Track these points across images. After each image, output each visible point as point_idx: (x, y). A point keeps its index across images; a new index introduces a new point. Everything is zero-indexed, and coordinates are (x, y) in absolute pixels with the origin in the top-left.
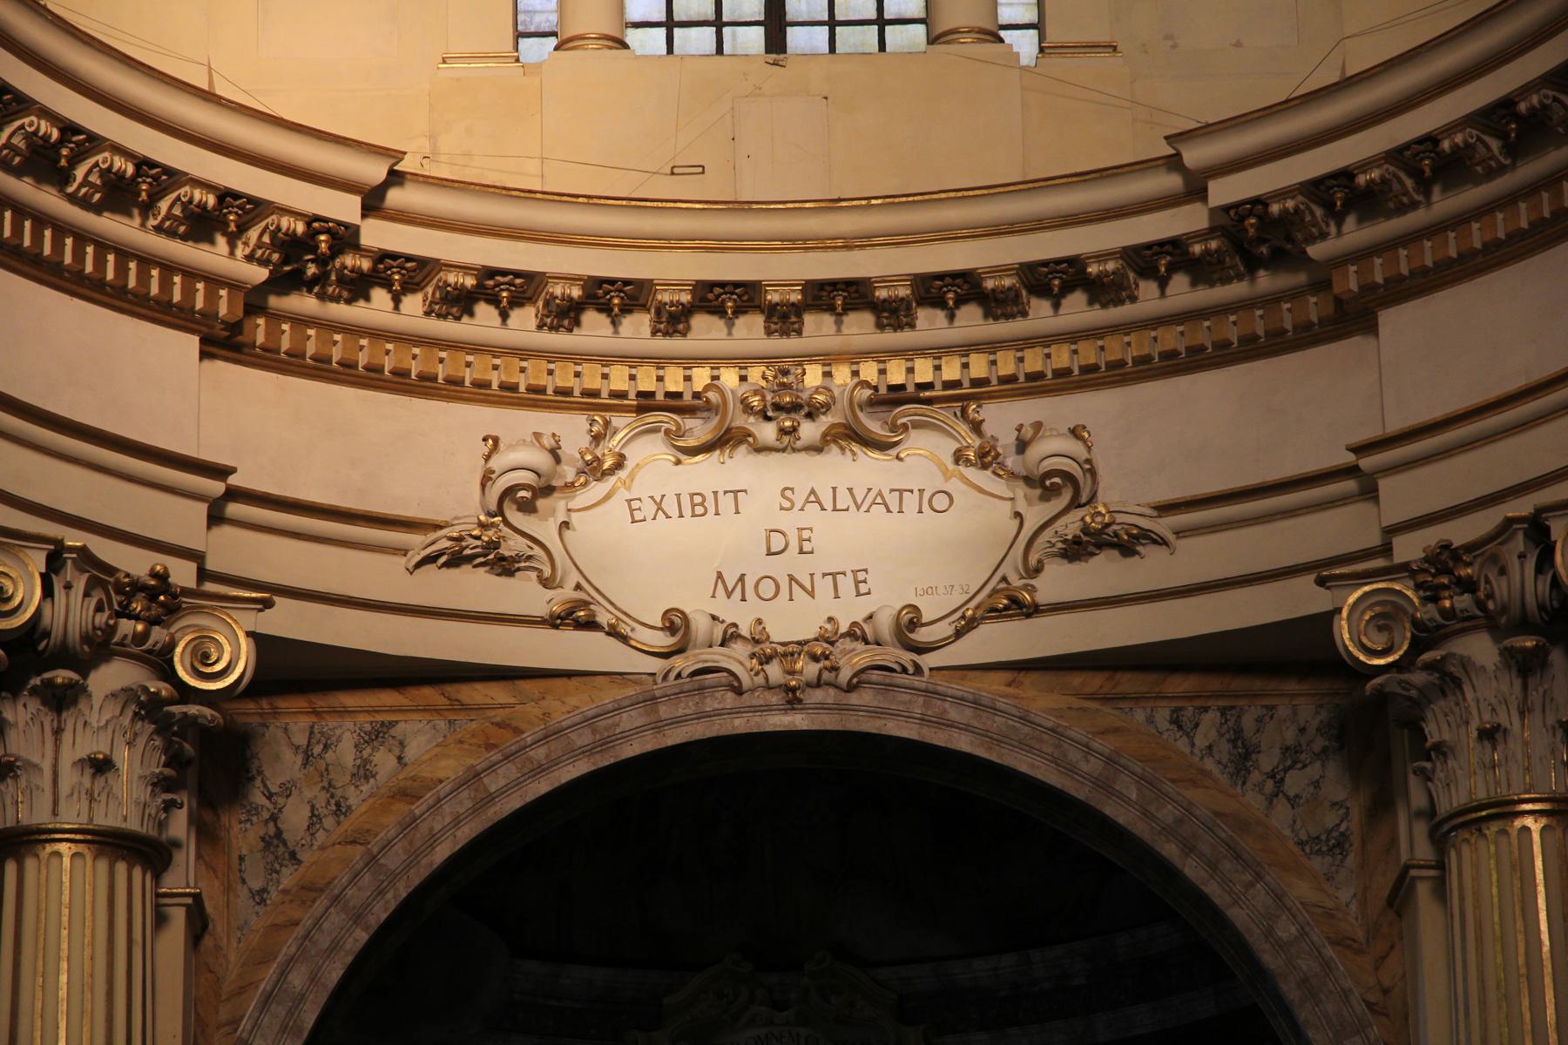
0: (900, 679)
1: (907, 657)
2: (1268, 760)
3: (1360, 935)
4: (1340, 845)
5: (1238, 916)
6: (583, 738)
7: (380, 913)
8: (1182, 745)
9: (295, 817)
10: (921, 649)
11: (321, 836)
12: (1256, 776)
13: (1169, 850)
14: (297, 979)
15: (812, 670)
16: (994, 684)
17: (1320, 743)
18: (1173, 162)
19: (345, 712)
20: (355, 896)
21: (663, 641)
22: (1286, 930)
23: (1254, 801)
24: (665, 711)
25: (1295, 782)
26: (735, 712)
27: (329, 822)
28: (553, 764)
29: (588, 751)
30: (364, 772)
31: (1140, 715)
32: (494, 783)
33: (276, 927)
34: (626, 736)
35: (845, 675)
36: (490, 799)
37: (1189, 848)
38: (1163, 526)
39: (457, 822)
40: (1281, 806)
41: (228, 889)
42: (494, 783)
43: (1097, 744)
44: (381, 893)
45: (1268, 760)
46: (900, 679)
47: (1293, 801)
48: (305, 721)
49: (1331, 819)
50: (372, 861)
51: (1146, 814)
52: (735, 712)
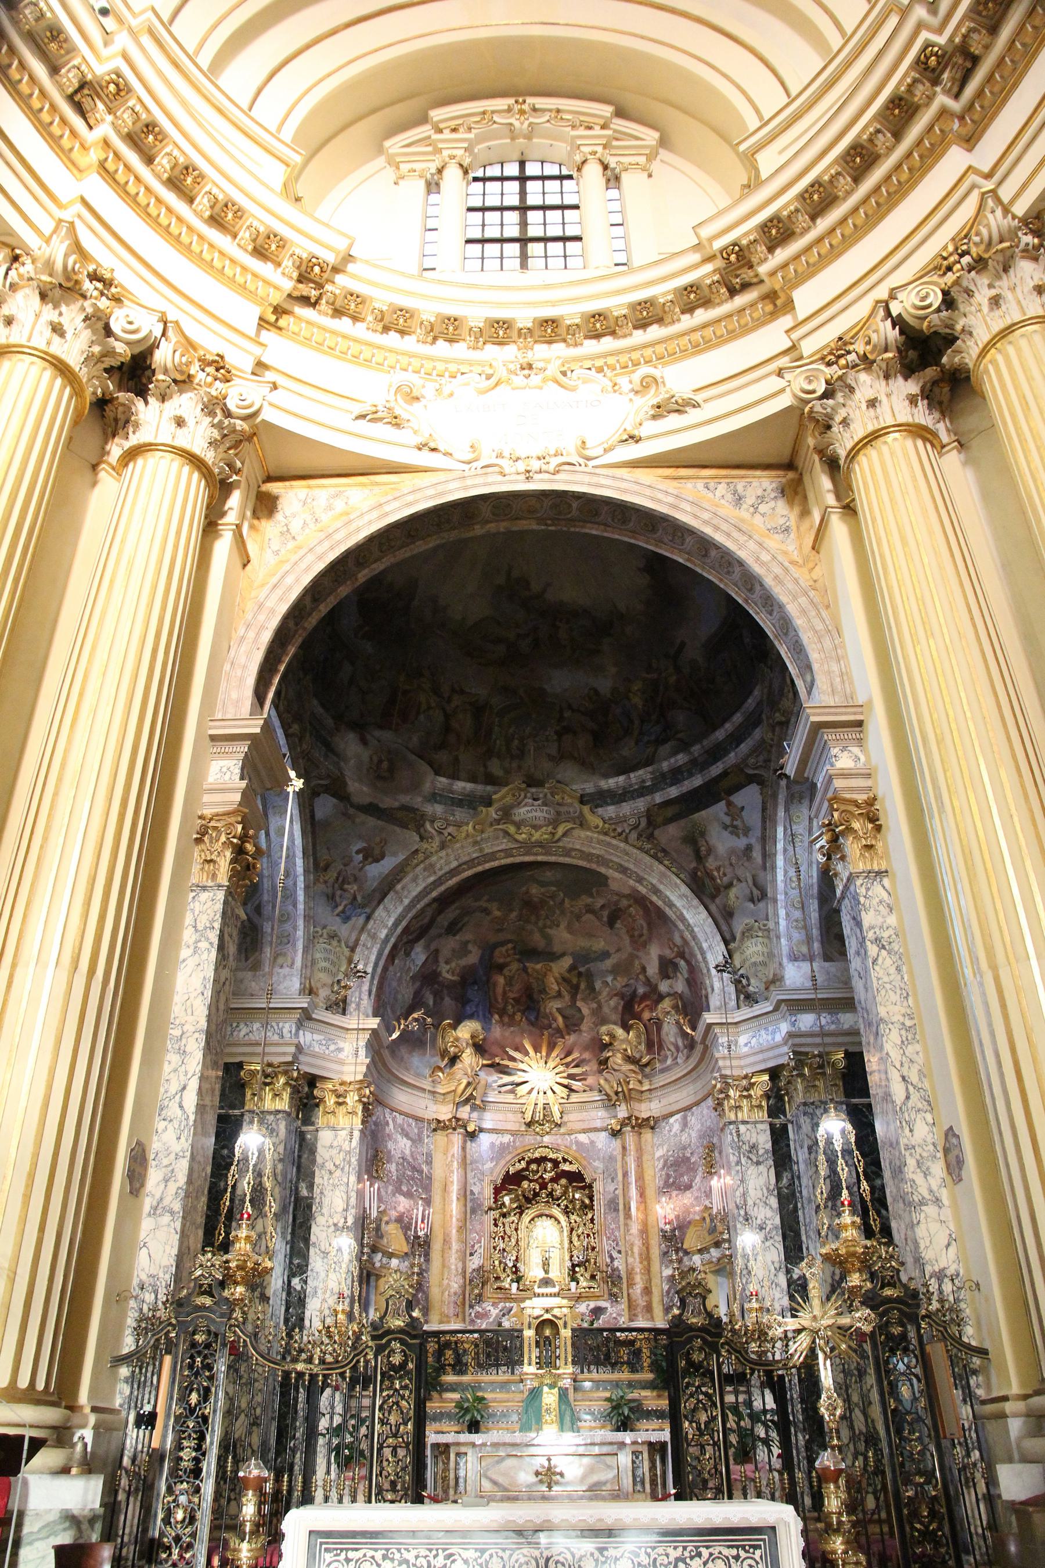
0: (577, 468)
1: (582, 461)
2: (750, 500)
3: (801, 562)
4: (787, 530)
5: (742, 554)
6: (431, 492)
7: (332, 556)
8: (710, 495)
9: (295, 526)
10: (589, 459)
11: (307, 531)
12: (745, 506)
13: (708, 530)
14: (289, 580)
15: (535, 465)
16: (623, 472)
17: (773, 495)
18: (698, 247)
19: (324, 486)
20: (320, 550)
21: (469, 456)
22: (765, 557)
23: (744, 513)
24: (469, 482)
25: (763, 508)
26: (500, 483)
27: (312, 525)
28: (417, 501)
29: (431, 497)
30: (330, 508)
31: (689, 485)
32: (387, 508)
33: (282, 562)
34: (450, 492)
35: (551, 468)
36: (387, 514)
37: (717, 528)
38: (699, 398)
39: (370, 522)
40: (757, 516)
41: (262, 549)
42: (387, 508)
43: (670, 491)
44: (332, 548)
45: (750, 500)
46: (577, 468)
47: (763, 515)
48: (306, 491)
49: (782, 521)
50: (328, 537)
51: (696, 517)
52: (500, 483)
